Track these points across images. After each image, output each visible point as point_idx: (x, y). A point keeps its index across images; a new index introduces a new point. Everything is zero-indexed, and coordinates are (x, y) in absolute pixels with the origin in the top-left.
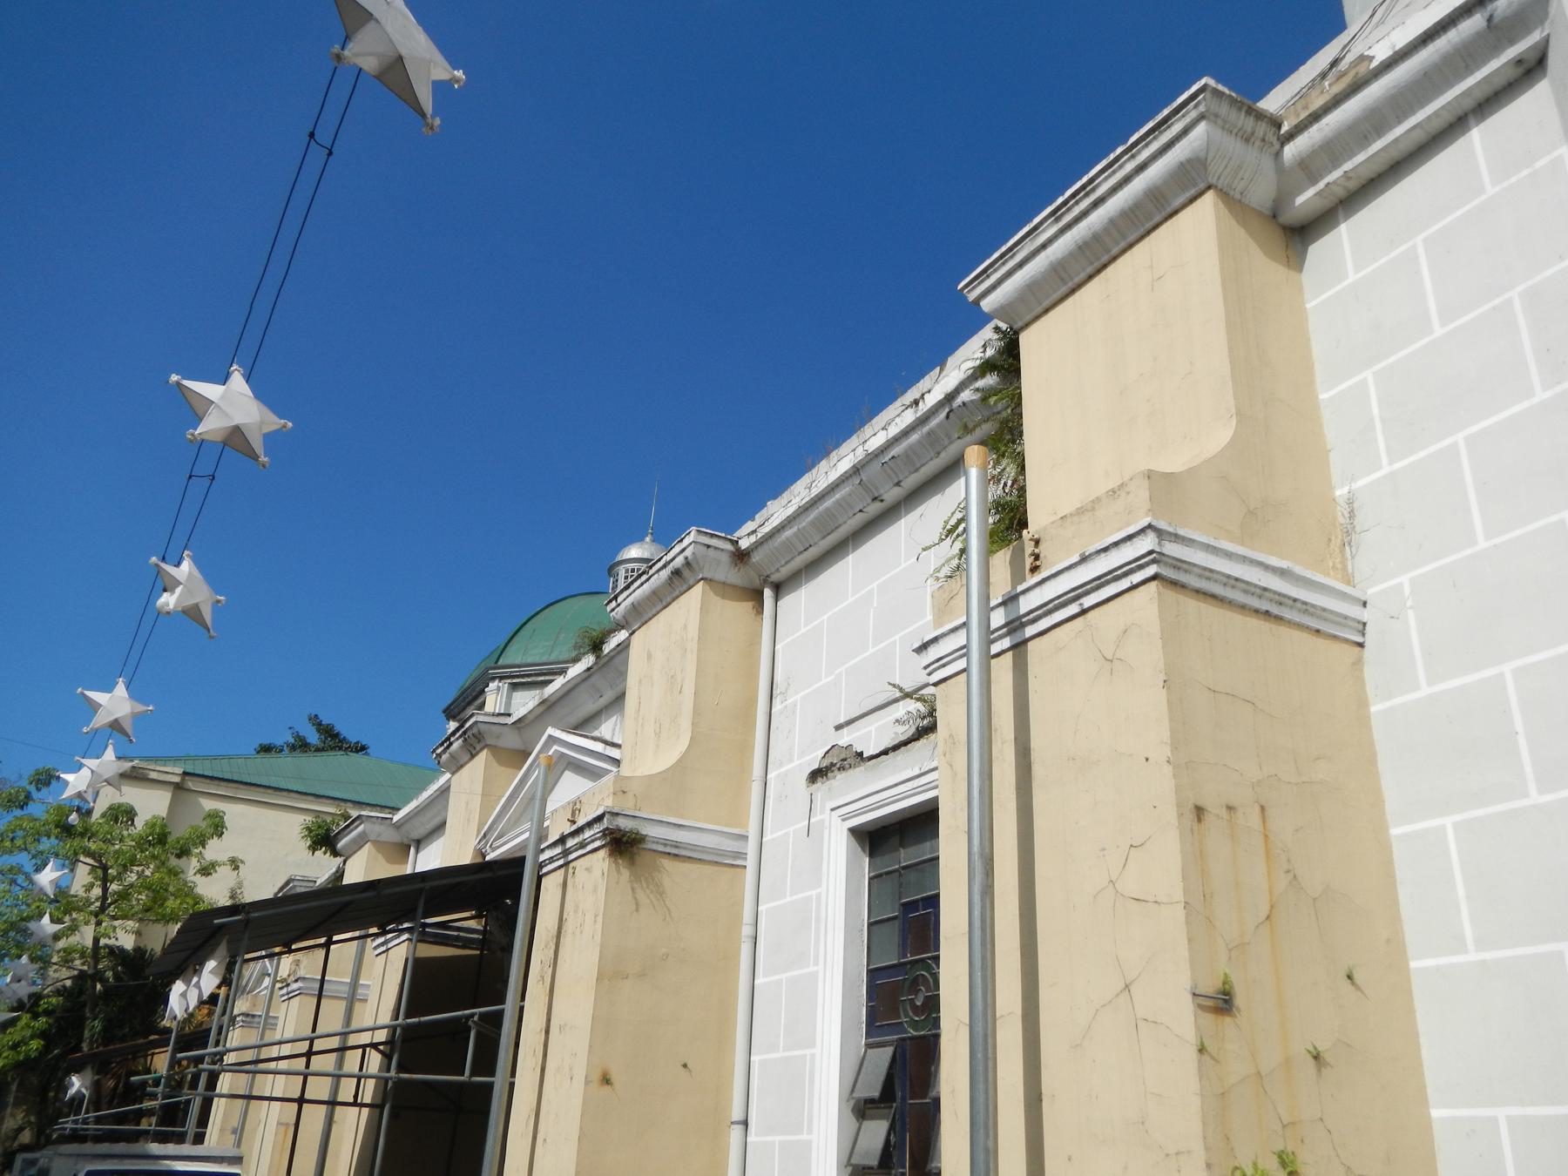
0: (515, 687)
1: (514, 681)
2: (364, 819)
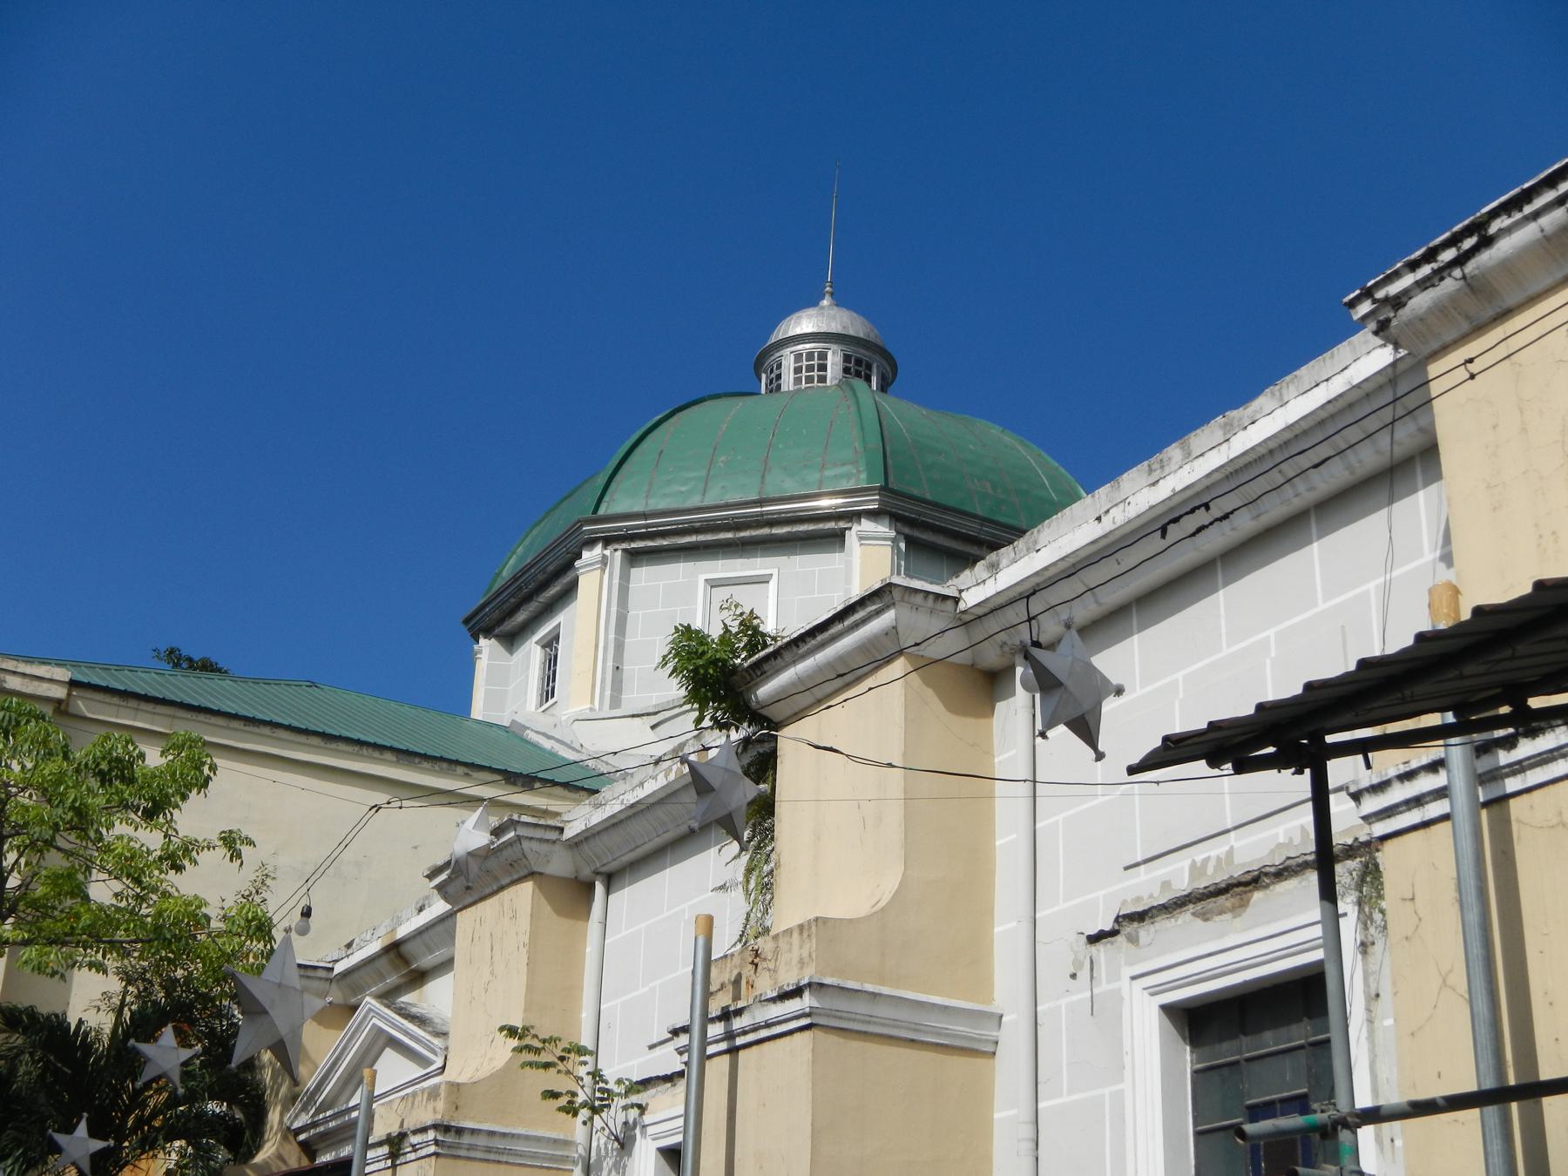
0: (634, 557)
1: (634, 545)
2: (896, 594)
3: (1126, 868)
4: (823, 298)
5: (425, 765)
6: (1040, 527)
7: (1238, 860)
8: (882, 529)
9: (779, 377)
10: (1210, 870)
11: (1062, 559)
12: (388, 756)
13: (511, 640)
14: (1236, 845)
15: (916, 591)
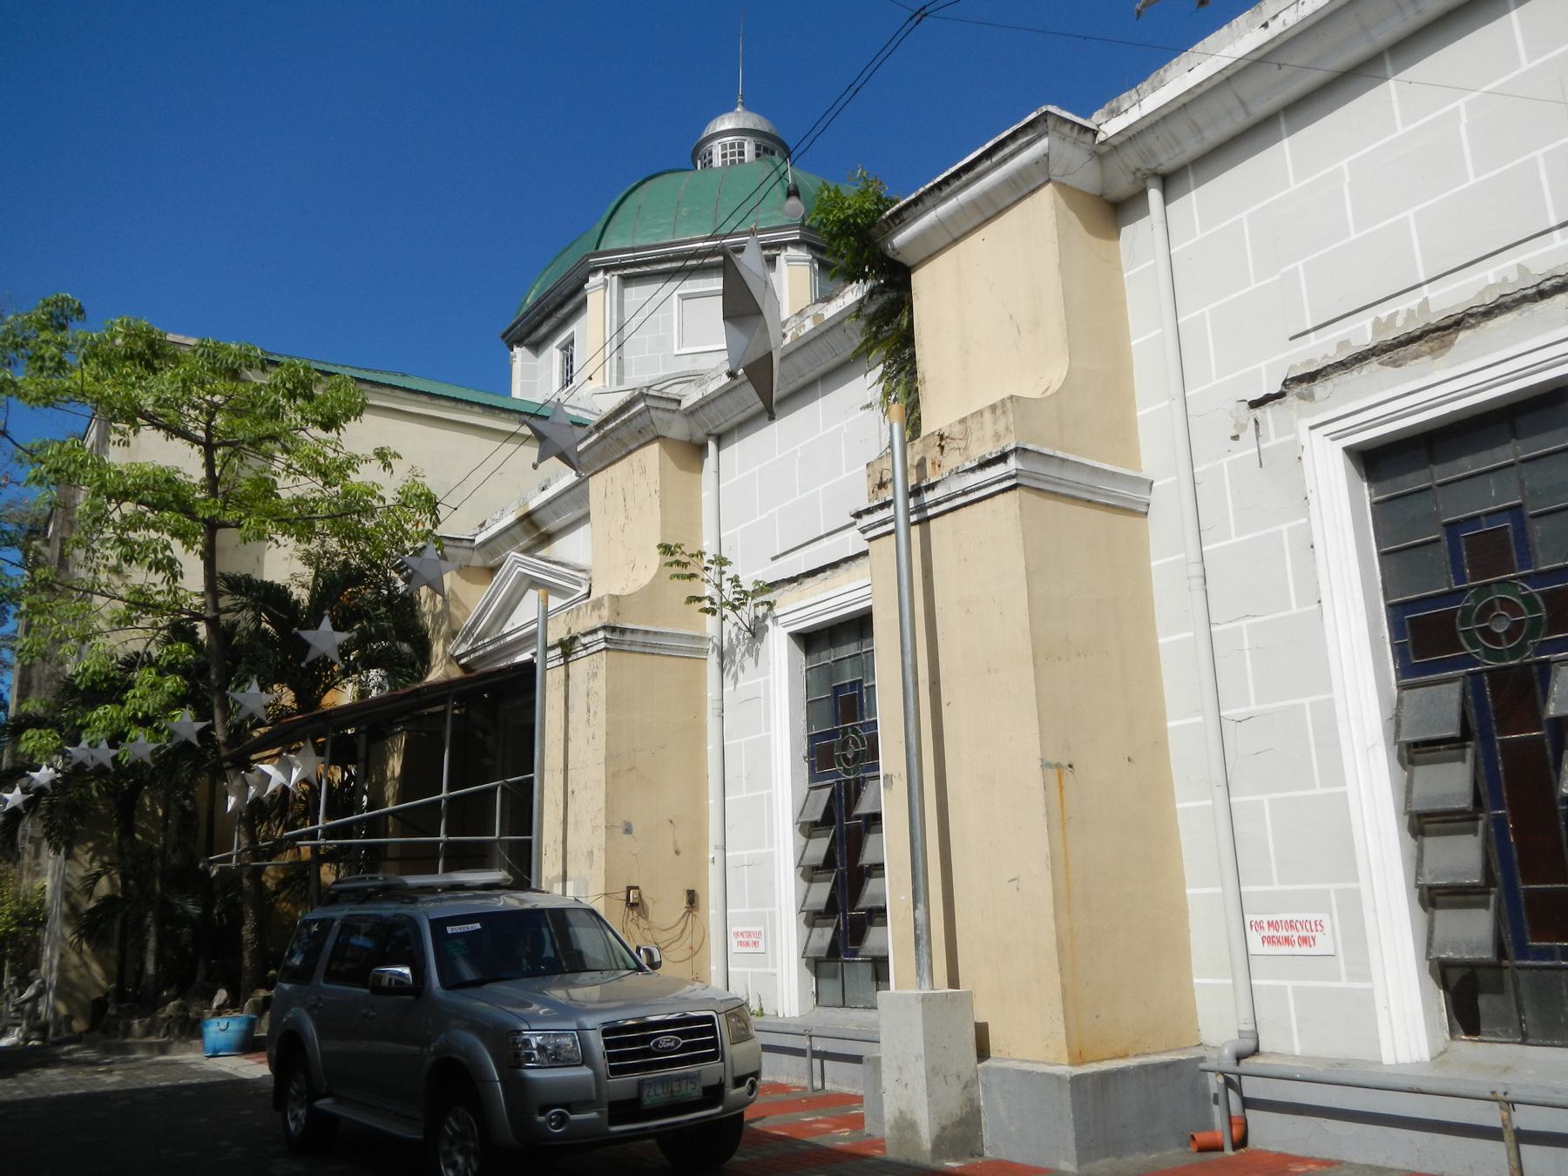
0: (626, 280)
2: (1050, 122)
3: (1291, 339)
4: (737, 107)
5: (503, 415)
6: (1166, 66)
7: (1433, 308)
8: (802, 254)
9: (711, 161)
10: (1399, 322)
11: (1220, 72)
12: (477, 409)
13: (537, 347)
14: (1431, 296)
15: (1066, 121)
